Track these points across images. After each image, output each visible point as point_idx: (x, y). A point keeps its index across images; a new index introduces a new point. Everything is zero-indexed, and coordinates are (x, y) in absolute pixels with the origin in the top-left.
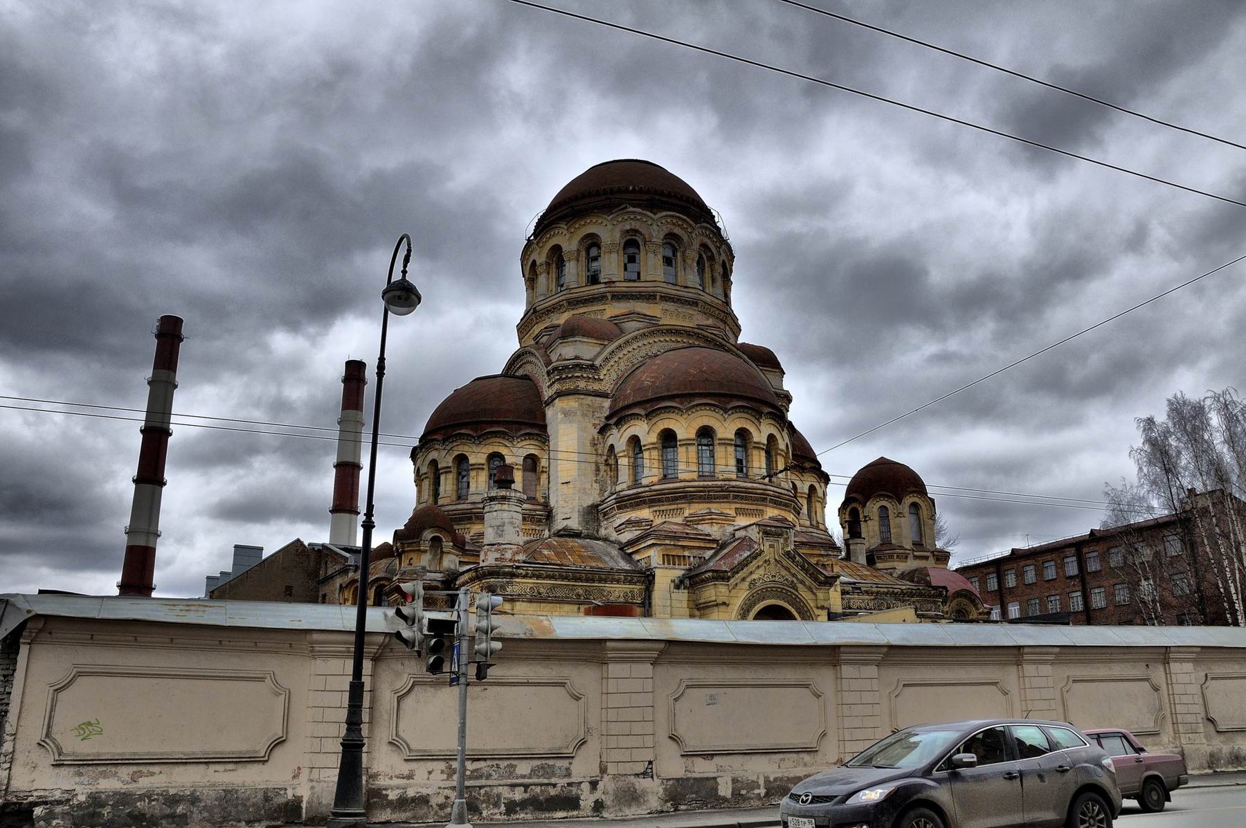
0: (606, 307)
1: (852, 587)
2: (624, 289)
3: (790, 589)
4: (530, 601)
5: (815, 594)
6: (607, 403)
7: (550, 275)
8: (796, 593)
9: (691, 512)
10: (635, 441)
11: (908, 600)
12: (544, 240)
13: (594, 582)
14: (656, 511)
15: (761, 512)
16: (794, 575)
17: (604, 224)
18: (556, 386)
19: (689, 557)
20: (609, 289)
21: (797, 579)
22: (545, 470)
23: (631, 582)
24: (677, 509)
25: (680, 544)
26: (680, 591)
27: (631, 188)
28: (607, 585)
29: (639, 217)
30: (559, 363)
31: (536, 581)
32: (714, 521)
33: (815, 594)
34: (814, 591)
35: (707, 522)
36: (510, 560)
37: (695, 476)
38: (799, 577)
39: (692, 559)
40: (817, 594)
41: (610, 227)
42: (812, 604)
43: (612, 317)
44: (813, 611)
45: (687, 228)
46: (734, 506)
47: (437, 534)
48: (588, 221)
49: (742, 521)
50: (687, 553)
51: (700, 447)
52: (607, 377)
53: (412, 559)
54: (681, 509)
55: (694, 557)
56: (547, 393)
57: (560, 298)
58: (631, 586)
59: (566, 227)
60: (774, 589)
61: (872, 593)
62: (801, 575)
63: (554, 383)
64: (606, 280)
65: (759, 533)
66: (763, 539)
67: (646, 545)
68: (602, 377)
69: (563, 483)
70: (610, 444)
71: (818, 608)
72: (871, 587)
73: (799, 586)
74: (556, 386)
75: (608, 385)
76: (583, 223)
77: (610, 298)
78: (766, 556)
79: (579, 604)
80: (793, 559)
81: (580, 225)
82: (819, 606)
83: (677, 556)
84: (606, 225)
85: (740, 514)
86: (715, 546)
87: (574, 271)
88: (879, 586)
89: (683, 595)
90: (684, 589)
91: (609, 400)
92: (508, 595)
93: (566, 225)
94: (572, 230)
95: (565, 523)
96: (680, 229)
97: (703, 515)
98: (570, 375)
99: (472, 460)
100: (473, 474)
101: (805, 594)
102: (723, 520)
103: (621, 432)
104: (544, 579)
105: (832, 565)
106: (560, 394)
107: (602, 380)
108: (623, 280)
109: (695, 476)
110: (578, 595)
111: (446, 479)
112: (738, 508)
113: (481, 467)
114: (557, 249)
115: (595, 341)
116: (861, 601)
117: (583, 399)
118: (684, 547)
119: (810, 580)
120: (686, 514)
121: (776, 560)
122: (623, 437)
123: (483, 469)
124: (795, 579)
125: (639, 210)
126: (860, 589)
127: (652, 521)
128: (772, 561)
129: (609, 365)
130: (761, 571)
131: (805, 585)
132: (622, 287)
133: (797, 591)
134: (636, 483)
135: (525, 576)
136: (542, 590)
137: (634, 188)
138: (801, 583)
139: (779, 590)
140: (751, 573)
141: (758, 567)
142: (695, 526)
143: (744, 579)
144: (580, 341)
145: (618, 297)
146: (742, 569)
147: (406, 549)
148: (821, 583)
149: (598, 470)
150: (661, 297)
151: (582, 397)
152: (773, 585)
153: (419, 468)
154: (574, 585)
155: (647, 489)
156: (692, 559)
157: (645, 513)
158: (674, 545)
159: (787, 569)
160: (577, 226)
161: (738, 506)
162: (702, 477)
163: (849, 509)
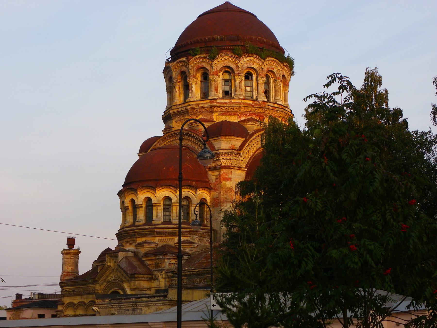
1: (173, 274)
11: (204, 277)
16: (123, 275)
28: (89, 286)
33: (130, 284)
40: (131, 283)
62: (125, 275)
79: (81, 295)
88: (185, 271)
105: (162, 263)
130: (111, 275)
140: (107, 277)
141: (110, 273)
150: (173, 115)
161: (126, 240)
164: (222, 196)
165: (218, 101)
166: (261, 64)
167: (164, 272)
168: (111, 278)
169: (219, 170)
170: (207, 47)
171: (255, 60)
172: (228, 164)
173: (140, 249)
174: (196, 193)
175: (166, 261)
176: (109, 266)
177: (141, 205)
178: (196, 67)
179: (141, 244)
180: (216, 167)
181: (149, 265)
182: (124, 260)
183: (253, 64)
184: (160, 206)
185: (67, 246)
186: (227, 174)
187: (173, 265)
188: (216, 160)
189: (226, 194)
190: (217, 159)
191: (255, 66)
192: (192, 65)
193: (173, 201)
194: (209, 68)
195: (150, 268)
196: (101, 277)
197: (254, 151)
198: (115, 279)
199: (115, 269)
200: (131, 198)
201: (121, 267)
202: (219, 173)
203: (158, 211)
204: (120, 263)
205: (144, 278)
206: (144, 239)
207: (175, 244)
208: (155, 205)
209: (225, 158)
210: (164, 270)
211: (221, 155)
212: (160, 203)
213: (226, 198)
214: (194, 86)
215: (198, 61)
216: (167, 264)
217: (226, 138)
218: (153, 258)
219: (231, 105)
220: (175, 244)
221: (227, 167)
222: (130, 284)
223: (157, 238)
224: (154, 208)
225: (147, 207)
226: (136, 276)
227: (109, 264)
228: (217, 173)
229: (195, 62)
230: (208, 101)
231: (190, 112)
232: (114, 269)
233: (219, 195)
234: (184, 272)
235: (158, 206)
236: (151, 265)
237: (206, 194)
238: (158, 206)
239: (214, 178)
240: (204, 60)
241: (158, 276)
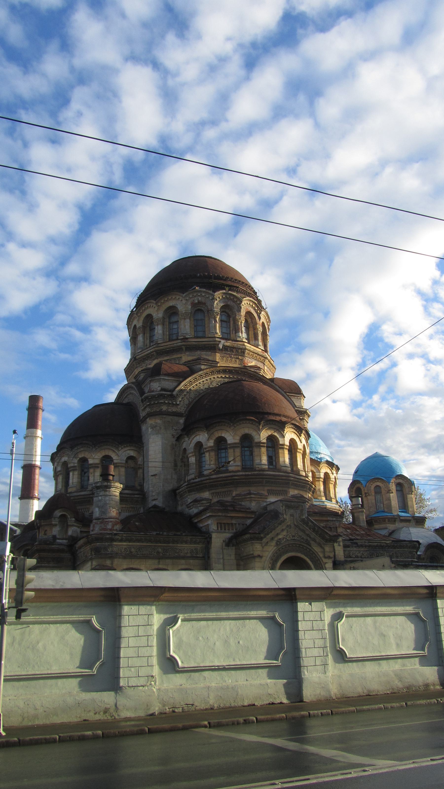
0: (182, 355)
2: (194, 343)
3: (305, 545)
4: (125, 558)
5: (323, 548)
6: (182, 421)
7: (146, 335)
8: (310, 548)
9: (238, 493)
10: (199, 445)
12: (141, 311)
13: (169, 543)
14: (214, 493)
15: (286, 492)
16: (308, 535)
17: (180, 300)
18: (148, 410)
19: (235, 524)
20: (183, 343)
21: (310, 537)
22: (141, 466)
23: (195, 543)
24: (228, 491)
25: (229, 515)
26: (230, 548)
27: (199, 275)
28: (179, 545)
29: (203, 294)
30: (149, 394)
31: (129, 544)
32: (252, 499)
34: (323, 546)
35: (248, 499)
36: (111, 530)
37: (239, 468)
38: (312, 536)
39: (237, 525)
41: (184, 302)
42: (321, 555)
43: (186, 362)
44: (322, 560)
45: (236, 301)
46: (266, 488)
47: (64, 513)
48: (170, 298)
49: (272, 499)
50: (234, 522)
51: (243, 449)
52: (182, 403)
53: (46, 530)
54: (230, 491)
55: (239, 524)
56: (142, 414)
57: (152, 350)
58: (195, 545)
59: (155, 302)
60: (294, 545)
61: (366, 546)
62: (313, 535)
63: (145, 408)
64: (182, 337)
65: (282, 507)
66: (285, 511)
67: (205, 516)
68: (178, 403)
69: (152, 476)
70: (184, 448)
71: (325, 557)
73: (312, 543)
74: (148, 410)
75: (183, 408)
76: (166, 299)
77: (184, 349)
78: (288, 522)
79: (159, 559)
80: (307, 524)
81: (164, 300)
82: (326, 556)
83: (227, 524)
84: (182, 300)
85: (273, 494)
86: (253, 516)
87: (160, 332)
89: (231, 552)
90: (233, 546)
91: (183, 418)
92: (109, 554)
93: (155, 300)
94: (159, 304)
95: (154, 503)
96: (232, 303)
97: (245, 495)
98: (156, 402)
99: (91, 461)
100: (91, 470)
101: (317, 549)
102: (259, 498)
103: (190, 440)
104: (134, 542)
106: (150, 415)
107: (178, 405)
108: (193, 337)
109: (239, 468)
110: (158, 552)
111: (73, 474)
112: (269, 490)
113: (97, 465)
114: (149, 316)
115: (173, 379)
116: (357, 552)
117: (165, 418)
118: (232, 517)
119: (319, 538)
120: (234, 494)
121: (295, 525)
122: (192, 443)
123: (98, 467)
124: (309, 539)
125: (204, 290)
126: (356, 543)
127: (211, 500)
128: (293, 526)
129: (183, 394)
130: (285, 533)
131: (315, 541)
132: (193, 341)
133: (310, 546)
134: (200, 474)
135: (121, 541)
136: (133, 550)
137: (200, 275)
138: (313, 541)
140: (278, 534)
141: (283, 530)
142: (240, 503)
143: (272, 539)
144: (163, 379)
145: (191, 348)
146: (271, 532)
147: (43, 524)
148: (327, 541)
149: (176, 465)
151: (164, 416)
152: (294, 543)
153: (56, 467)
154: (155, 546)
155: (207, 478)
156: (237, 525)
157: (206, 495)
158: (225, 516)
159: (303, 531)
160: (162, 301)
161: (269, 488)
162: (244, 468)
163: (355, 488)
200: (270, 434)
218: (325, 519)
222: (323, 548)
240: (254, 306)
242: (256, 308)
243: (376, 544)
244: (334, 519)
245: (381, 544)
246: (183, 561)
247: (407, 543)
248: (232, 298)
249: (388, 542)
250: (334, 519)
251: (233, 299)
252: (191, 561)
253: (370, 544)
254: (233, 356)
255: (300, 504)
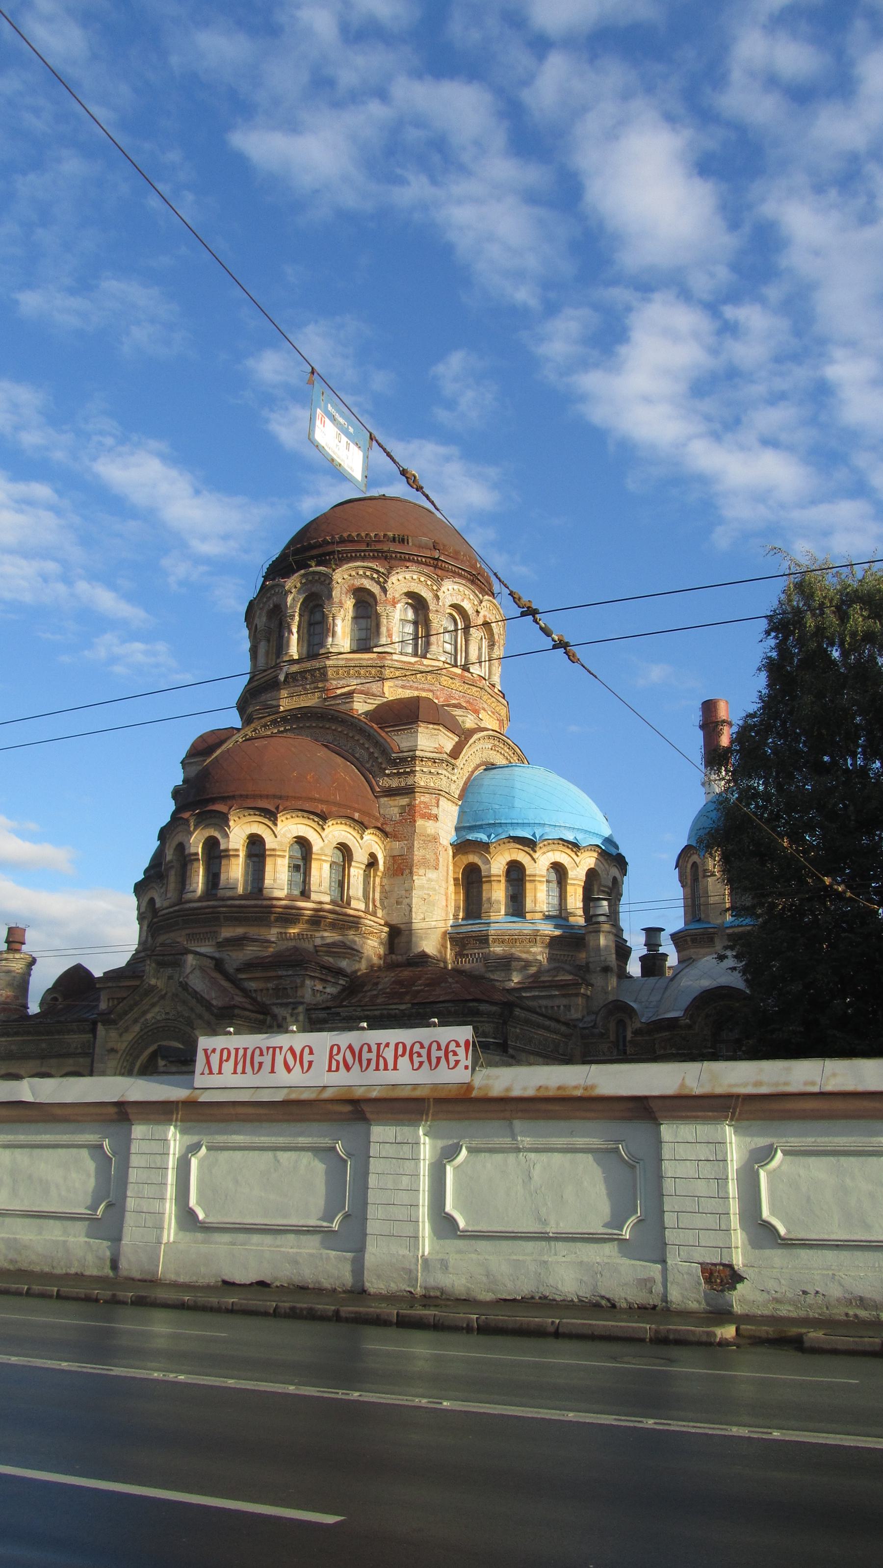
16: (192, 1009)
28: (66, 1037)
31: (8, 1039)
62: (200, 1009)
72: (355, 1010)
88: (365, 1008)
126: (338, 1014)
130: (157, 1009)
139: (150, 1033)
140: (145, 1013)
141: (153, 1005)
161: (188, 931)
164: (416, 853)
165: (395, 657)
166: (476, 603)
167: (301, 1009)
168: (154, 1014)
169: (412, 795)
170: (371, 551)
171: (467, 592)
172: (432, 785)
173: (230, 953)
174: (362, 838)
175: (308, 982)
176: (153, 988)
177: (237, 850)
178: (346, 586)
179: (238, 942)
180: (403, 788)
181: (255, 991)
182: (197, 973)
183: (463, 600)
184: (284, 857)
185: (6, 944)
186: (427, 806)
187: (318, 995)
188: (405, 773)
189: (425, 849)
190: (408, 770)
191: (467, 605)
192: (339, 581)
193: (315, 849)
194: (376, 589)
195: (259, 999)
196: (126, 1013)
197: (470, 770)
198: (169, 1019)
199: (169, 994)
201: (190, 990)
202: (411, 802)
203: (279, 868)
204: (188, 978)
205: (250, 1020)
206: (239, 931)
207: (315, 946)
208: (273, 853)
209: (425, 770)
210: (302, 1003)
211: (417, 762)
212: (285, 851)
213: (424, 858)
214: (339, 622)
215: (354, 573)
216: (310, 990)
217: (428, 728)
218: (272, 974)
219: (422, 668)
220: (318, 948)
221: (428, 790)
223: (275, 930)
224: (269, 862)
225: (250, 855)
226: (237, 1011)
227: (153, 982)
228: (404, 801)
229: (346, 576)
230: (374, 656)
231: (329, 673)
232: (166, 994)
233: (408, 849)
234: (363, 1010)
235: (279, 856)
236: (261, 990)
237: (377, 846)
238: (279, 856)
239: (396, 810)
240: (368, 573)
241: (285, 1019)
242: (375, 576)
243: (379, 1012)
244: (290, 973)
245: (390, 1012)
246: (71, 1061)
247: (449, 1005)
248: (317, 577)
249: (403, 1007)
250: (290, 973)
251: (319, 579)
252: (81, 1060)
253: (366, 1013)
254: (308, 687)
255: (176, 957)
